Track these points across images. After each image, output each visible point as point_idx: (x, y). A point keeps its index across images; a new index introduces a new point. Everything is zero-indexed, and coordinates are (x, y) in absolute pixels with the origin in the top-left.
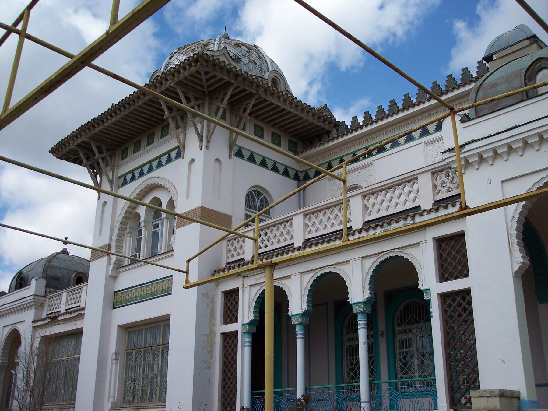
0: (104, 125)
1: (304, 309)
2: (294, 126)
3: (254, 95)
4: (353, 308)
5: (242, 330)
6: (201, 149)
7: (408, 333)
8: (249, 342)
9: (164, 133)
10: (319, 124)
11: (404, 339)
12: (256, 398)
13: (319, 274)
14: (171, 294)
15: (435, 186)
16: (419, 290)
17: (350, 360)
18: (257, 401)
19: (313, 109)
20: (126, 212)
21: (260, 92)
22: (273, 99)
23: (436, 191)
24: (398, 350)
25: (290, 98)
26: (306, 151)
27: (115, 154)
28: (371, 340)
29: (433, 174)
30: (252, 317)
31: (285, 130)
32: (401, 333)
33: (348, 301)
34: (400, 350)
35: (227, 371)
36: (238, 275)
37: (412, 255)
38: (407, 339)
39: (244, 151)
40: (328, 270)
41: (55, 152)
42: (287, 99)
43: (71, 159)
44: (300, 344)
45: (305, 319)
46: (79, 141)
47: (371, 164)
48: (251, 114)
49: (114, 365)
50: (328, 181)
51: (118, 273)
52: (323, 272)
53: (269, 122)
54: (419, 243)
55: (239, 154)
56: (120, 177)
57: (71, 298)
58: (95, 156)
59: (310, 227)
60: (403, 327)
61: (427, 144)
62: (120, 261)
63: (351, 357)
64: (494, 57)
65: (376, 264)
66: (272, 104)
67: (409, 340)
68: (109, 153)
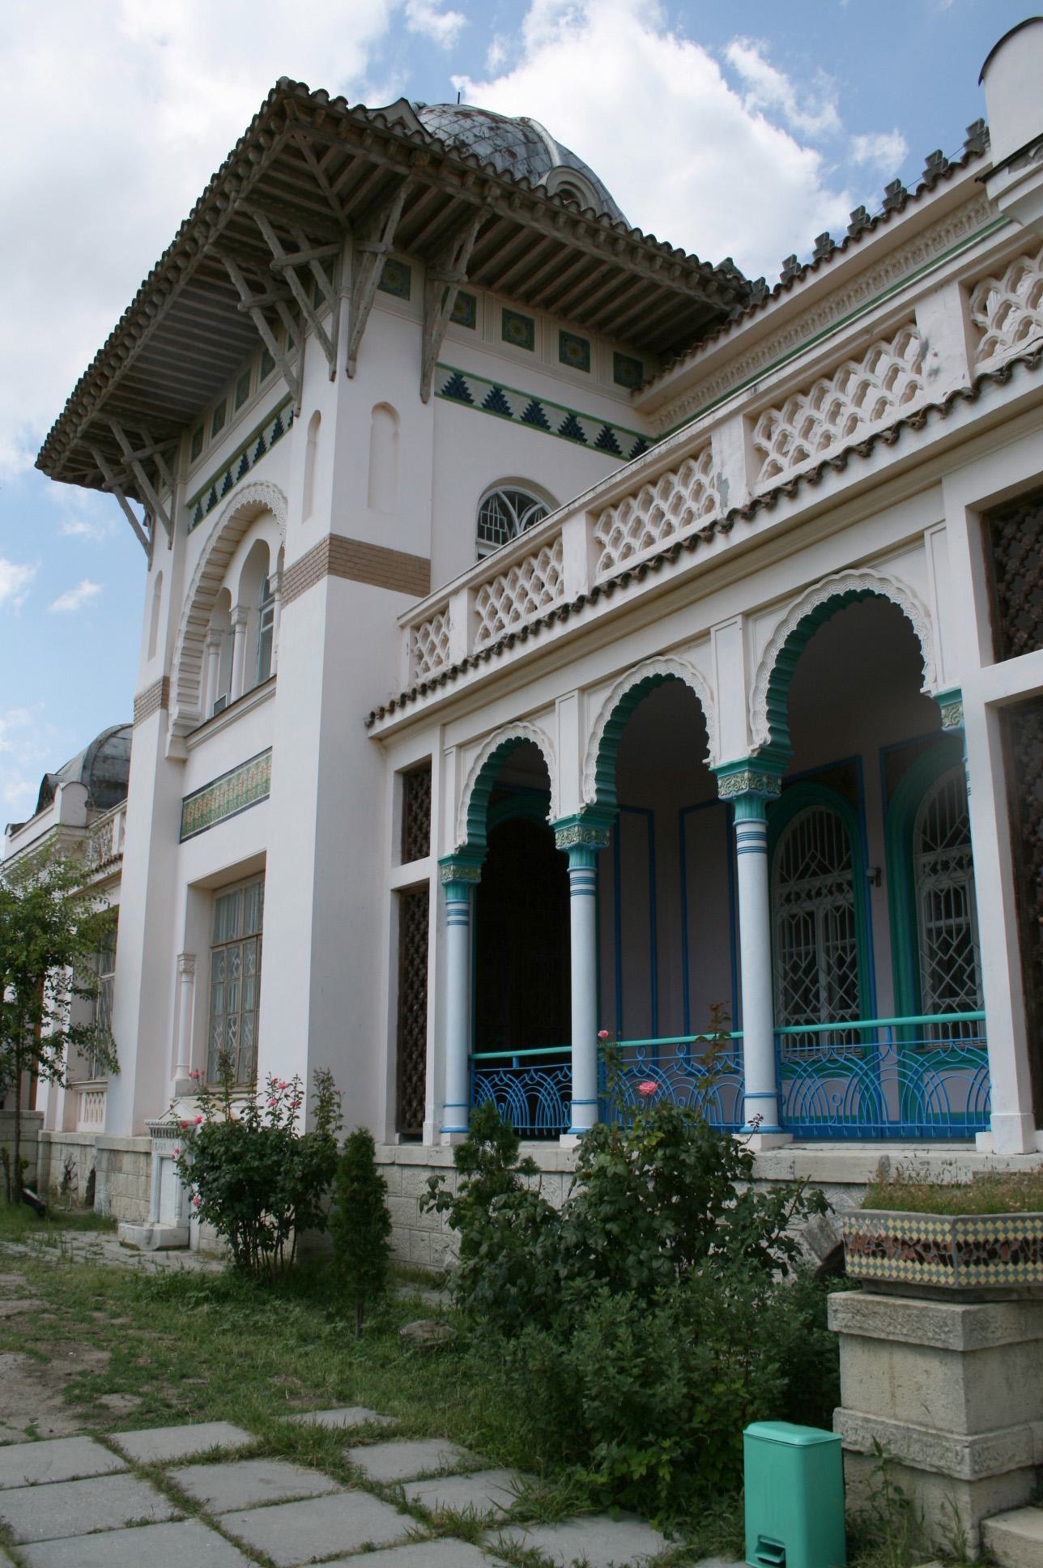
2: (620, 311)
3: (478, 209)
4: (720, 782)
5: (440, 877)
7: (955, 869)
8: (459, 912)
9: (268, 364)
10: (692, 293)
11: (941, 891)
12: (482, 1074)
13: (626, 688)
15: (977, 330)
16: (925, 698)
17: (791, 956)
19: (666, 247)
21: (489, 200)
22: (536, 220)
23: (981, 346)
24: (925, 923)
25: (589, 215)
26: (661, 377)
27: (176, 447)
28: (848, 896)
29: (969, 288)
30: (463, 839)
31: (600, 325)
32: (934, 870)
33: (705, 761)
34: (933, 925)
35: (411, 997)
38: (949, 891)
39: (472, 387)
40: (649, 672)
42: (579, 218)
43: (88, 480)
44: (580, 909)
45: (593, 833)
48: (471, 271)
49: (184, 988)
51: (189, 750)
52: (637, 679)
53: (548, 303)
55: (457, 391)
56: (190, 506)
58: (123, 454)
59: (609, 549)
62: (193, 719)
65: (786, 633)
67: (956, 891)
68: (160, 447)
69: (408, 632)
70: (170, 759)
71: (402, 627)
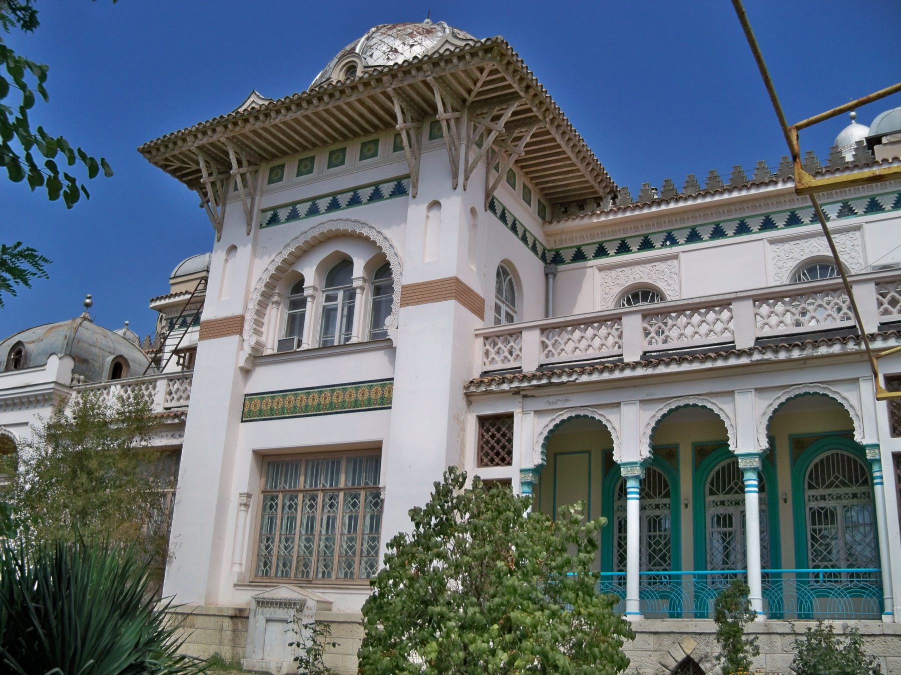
0: (267, 122)
1: (644, 457)
2: (553, 181)
3: (540, 121)
6: (455, 189)
14: (390, 408)
18: (802, 587)
20: (278, 269)
21: (547, 119)
36: (517, 392)
37: (847, 396)
38: (725, 515)
41: (149, 152)
46: (205, 141)
47: (676, 257)
50: (597, 271)
54: (858, 379)
56: (264, 211)
57: (129, 395)
60: (721, 497)
61: (772, 242)
63: (658, 533)
64: (884, 140)
66: (554, 140)
69: (481, 340)
70: (241, 368)
71: (476, 335)
